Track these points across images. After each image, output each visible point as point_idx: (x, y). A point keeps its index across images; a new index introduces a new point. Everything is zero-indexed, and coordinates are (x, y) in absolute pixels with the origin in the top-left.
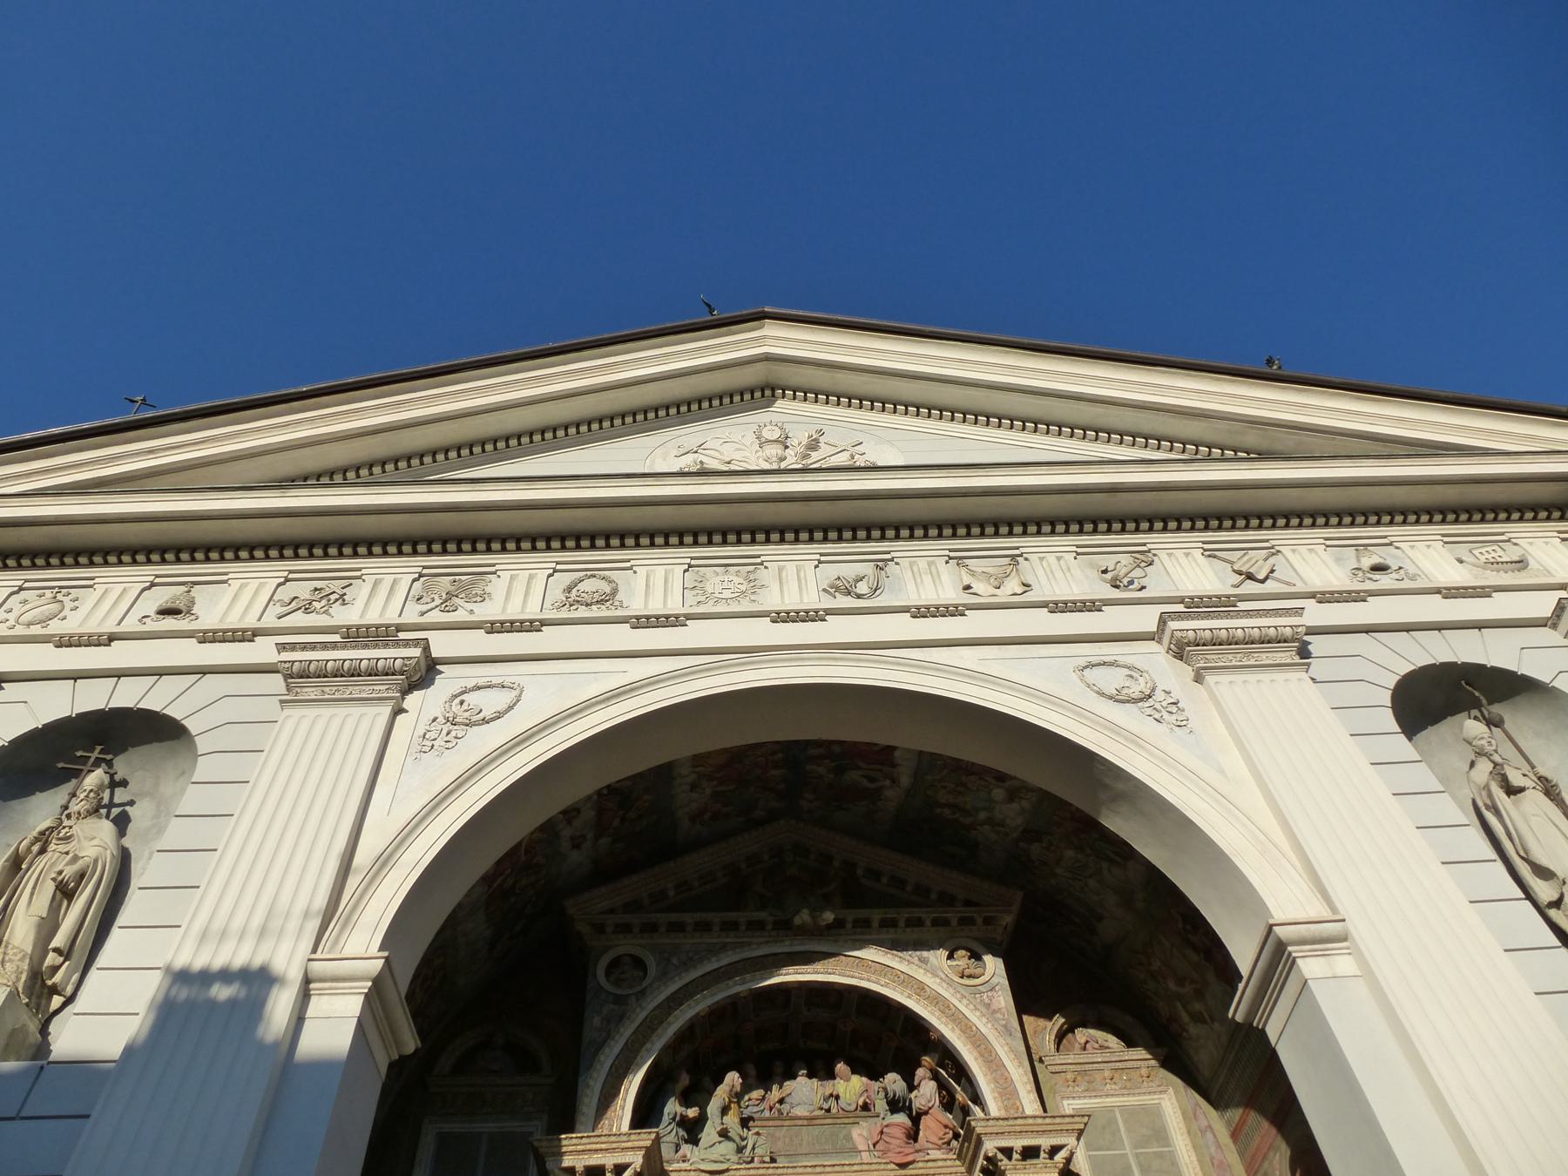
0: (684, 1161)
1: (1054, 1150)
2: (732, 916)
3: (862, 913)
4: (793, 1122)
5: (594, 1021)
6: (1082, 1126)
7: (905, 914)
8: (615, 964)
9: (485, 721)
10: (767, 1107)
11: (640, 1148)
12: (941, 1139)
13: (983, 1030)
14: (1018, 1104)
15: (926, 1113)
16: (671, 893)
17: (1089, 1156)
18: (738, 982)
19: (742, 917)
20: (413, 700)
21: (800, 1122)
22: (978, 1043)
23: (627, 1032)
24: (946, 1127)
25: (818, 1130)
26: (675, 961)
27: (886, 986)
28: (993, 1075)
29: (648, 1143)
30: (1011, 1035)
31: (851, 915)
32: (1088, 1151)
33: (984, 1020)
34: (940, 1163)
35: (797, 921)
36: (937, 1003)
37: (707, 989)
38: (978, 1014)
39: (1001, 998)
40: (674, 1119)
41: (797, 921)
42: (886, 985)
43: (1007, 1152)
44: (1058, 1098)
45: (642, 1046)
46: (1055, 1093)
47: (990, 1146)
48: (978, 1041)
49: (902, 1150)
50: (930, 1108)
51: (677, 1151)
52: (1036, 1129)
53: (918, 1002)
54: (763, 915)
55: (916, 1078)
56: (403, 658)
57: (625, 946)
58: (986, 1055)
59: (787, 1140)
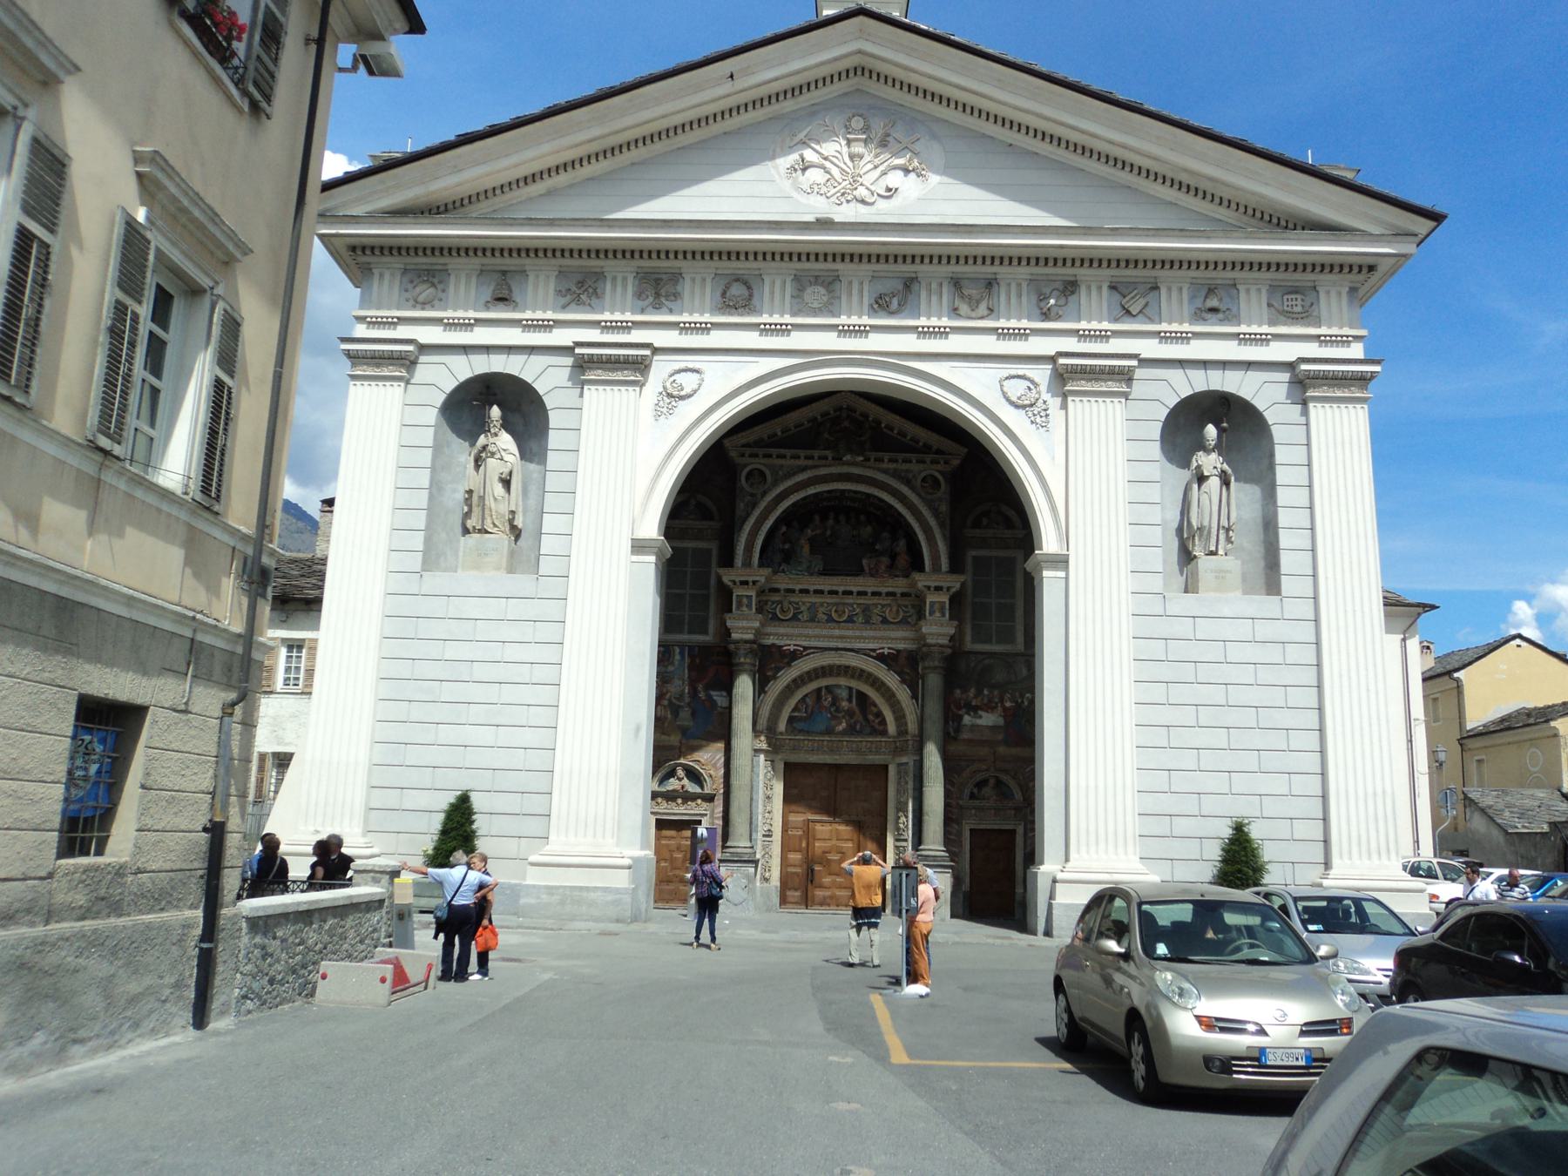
1: (948, 589)
2: (809, 452)
3: (880, 454)
5: (741, 506)
7: (901, 456)
8: (750, 474)
9: (689, 396)
16: (779, 434)
19: (816, 453)
23: (756, 513)
26: (780, 473)
31: (873, 455)
41: (844, 459)
47: (920, 585)
54: (827, 453)
57: (756, 464)
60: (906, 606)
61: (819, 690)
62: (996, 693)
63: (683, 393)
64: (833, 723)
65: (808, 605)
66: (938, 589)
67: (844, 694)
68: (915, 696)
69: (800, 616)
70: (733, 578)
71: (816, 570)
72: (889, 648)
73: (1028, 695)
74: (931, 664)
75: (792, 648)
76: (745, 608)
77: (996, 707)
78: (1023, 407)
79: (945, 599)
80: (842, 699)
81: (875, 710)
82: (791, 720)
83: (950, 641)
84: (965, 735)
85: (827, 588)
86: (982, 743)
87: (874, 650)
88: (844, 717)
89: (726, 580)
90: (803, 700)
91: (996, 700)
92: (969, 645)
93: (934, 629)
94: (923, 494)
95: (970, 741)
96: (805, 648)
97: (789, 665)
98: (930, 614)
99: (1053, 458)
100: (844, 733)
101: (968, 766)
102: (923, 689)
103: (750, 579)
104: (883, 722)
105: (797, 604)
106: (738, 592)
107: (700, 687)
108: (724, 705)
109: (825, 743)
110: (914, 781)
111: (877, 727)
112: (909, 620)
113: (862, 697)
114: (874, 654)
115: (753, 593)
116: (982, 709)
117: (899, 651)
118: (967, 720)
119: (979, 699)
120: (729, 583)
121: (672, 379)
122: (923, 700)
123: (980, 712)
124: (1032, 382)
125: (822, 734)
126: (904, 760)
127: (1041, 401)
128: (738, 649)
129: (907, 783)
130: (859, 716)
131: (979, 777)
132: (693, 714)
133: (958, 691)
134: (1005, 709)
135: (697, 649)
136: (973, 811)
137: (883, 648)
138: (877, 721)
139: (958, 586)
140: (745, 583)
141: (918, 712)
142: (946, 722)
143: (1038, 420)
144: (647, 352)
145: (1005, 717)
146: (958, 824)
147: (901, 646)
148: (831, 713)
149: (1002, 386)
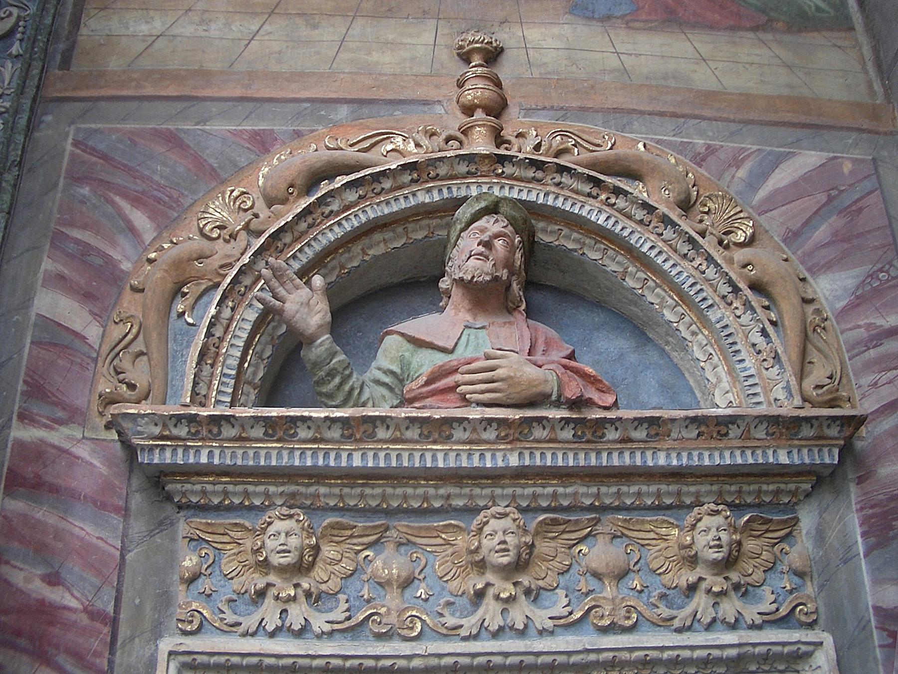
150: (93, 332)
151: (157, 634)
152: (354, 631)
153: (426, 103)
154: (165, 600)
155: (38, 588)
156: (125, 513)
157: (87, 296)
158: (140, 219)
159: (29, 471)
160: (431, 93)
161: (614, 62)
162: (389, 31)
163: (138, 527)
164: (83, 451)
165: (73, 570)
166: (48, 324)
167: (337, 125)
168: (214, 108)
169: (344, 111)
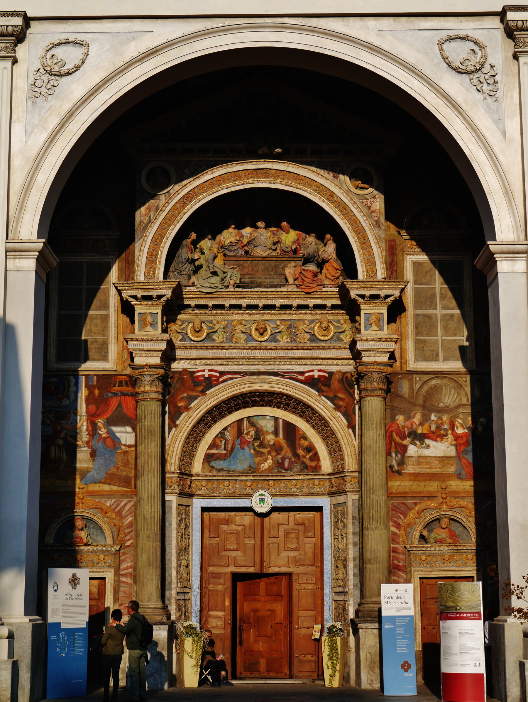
0: (193, 286)
1: (387, 297)
4: (254, 259)
6: (403, 286)
9: (69, 73)
10: (241, 247)
11: (170, 288)
12: (333, 276)
13: (363, 224)
14: (374, 269)
15: (327, 261)
17: (415, 288)
18: (225, 188)
20: (21, 51)
21: (258, 259)
22: (359, 231)
24: (337, 270)
25: (268, 263)
26: (186, 171)
27: (310, 194)
28: (364, 251)
29: (174, 286)
30: (379, 227)
32: (415, 284)
33: (365, 218)
34: (329, 293)
35: (260, 152)
36: (339, 205)
37: (206, 191)
38: (362, 214)
39: (378, 203)
40: (187, 261)
42: (310, 193)
43: (363, 297)
44: (405, 255)
45: (169, 226)
46: (404, 252)
48: (359, 231)
49: (309, 285)
50: (330, 260)
51: (189, 280)
52: (379, 286)
53: (328, 205)
55: (326, 239)
56: (12, 26)
58: (362, 240)
59: (250, 268)
60: (338, 321)
61: (240, 421)
62: (445, 418)
63: (64, 70)
64: (257, 460)
65: (223, 323)
66: (374, 297)
67: (268, 425)
68: (351, 426)
69: (214, 337)
70: (134, 293)
71: (232, 282)
72: (319, 371)
73: (482, 420)
74: (369, 386)
75: (206, 374)
76: (149, 328)
77: (446, 435)
78: (468, 73)
79: (382, 309)
80: (267, 433)
81: (306, 444)
82: (208, 458)
83: (390, 358)
84: (410, 469)
85: (244, 303)
86: (431, 477)
87: (302, 373)
88: (269, 452)
89: (125, 295)
90: (222, 433)
91: (446, 426)
92: (412, 365)
93: (371, 345)
94: (353, 190)
95: (416, 476)
96: (222, 374)
97: (203, 392)
98: (366, 328)
99: (504, 133)
100: (270, 470)
101: (416, 504)
102: (361, 416)
103: (154, 293)
104: (316, 457)
105: (211, 322)
106: (140, 309)
107: (100, 422)
108: (129, 443)
109: (249, 483)
110: (353, 524)
111: (308, 462)
112: (342, 336)
113: (290, 428)
114: (303, 378)
115: (158, 310)
116: (428, 438)
117: (331, 374)
118: (412, 450)
119: (427, 425)
120: (130, 299)
121: (49, 55)
122: (361, 429)
123: (427, 441)
124: (476, 43)
125: (245, 473)
126: (341, 499)
127: (487, 67)
128: (143, 375)
129: (345, 526)
130: (287, 451)
131: (428, 517)
132: (93, 454)
133: (400, 419)
134: (457, 437)
135: (95, 377)
136: (423, 557)
137: (313, 371)
138: (308, 457)
139: (397, 294)
140: (148, 298)
141: (356, 443)
142: (389, 454)
143: (485, 87)
144: (18, 21)
145: (456, 446)
146: (406, 572)
147: (333, 367)
148: (254, 449)
149: (441, 50)
150: (398, 533)
151: (410, 567)
152: (431, 567)
153: (437, 497)
154: (411, 564)
155: (397, 563)
156: (405, 554)
157: (397, 528)
158: (401, 516)
159: (394, 550)
160: (437, 495)
161: (463, 487)
162: (432, 483)
163: (407, 556)
164: (400, 548)
165: (401, 561)
166: (393, 532)
167: (425, 501)
168: (409, 498)
169: (426, 498)
